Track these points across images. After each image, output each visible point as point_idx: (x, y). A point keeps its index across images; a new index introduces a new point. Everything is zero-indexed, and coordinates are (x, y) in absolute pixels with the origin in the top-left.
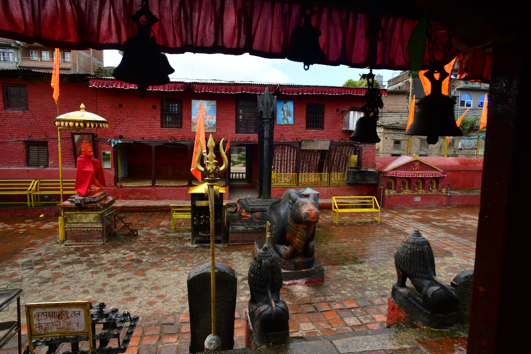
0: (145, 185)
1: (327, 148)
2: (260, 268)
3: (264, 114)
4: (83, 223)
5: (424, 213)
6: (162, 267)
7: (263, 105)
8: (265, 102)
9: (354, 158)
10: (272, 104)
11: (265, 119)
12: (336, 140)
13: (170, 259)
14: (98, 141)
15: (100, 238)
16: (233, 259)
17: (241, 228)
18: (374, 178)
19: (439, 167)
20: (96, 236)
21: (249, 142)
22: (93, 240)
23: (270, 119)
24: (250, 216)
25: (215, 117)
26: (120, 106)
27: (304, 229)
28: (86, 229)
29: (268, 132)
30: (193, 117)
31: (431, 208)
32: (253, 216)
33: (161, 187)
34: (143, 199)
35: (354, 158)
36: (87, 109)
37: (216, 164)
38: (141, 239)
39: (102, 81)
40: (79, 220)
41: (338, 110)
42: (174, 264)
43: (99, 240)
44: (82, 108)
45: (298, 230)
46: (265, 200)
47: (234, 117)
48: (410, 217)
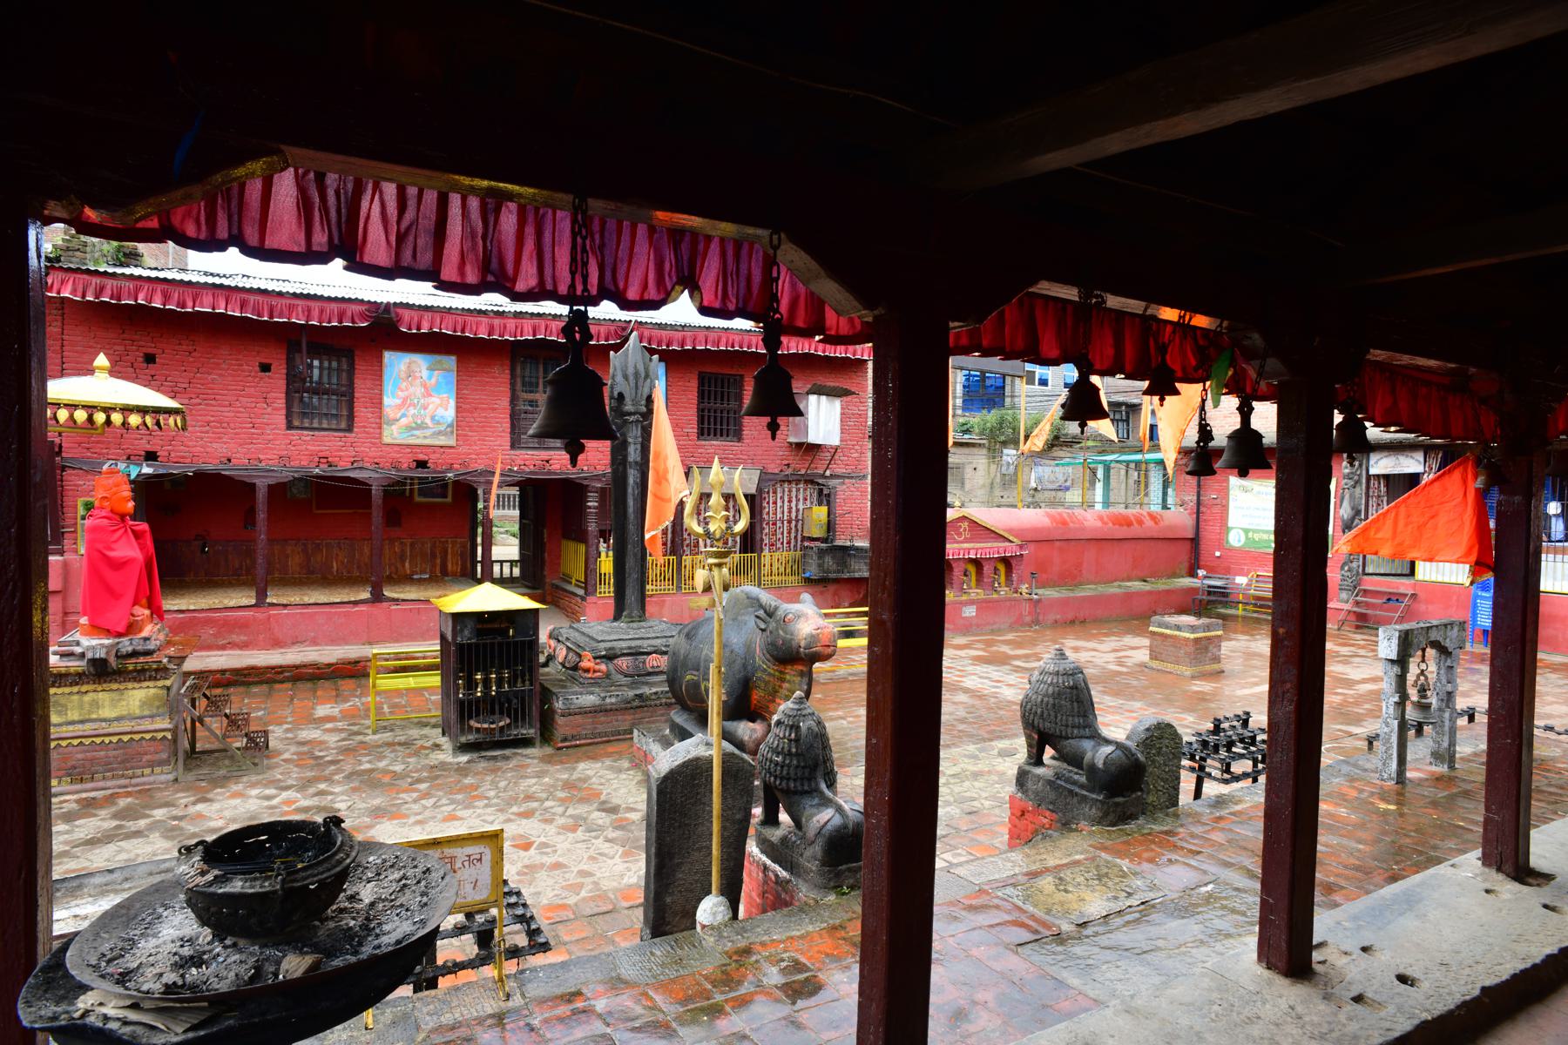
0: (232, 603)
2: (797, 740)
3: (628, 400)
4: (104, 720)
5: (989, 643)
6: (406, 816)
7: (626, 377)
8: (631, 371)
9: (821, 512)
10: (647, 376)
11: (630, 414)
12: (774, 468)
13: (415, 795)
14: (63, 468)
15: (161, 763)
16: (590, 778)
17: (589, 700)
19: (1010, 531)
20: (146, 758)
21: (549, 473)
22: (139, 772)
24: (603, 667)
25: (452, 403)
26: (150, 359)
27: (802, 674)
28: (115, 739)
30: (388, 401)
31: (999, 632)
32: (611, 666)
33: (285, 606)
34: (223, 648)
35: (821, 512)
36: (114, 372)
37: (727, 519)
38: (286, 756)
39: (96, 280)
40: (90, 712)
42: (435, 806)
43: (157, 770)
44: (102, 369)
45: (783, 680)
46: (635, 625)
47: (504, 403)
48: (962, 653)
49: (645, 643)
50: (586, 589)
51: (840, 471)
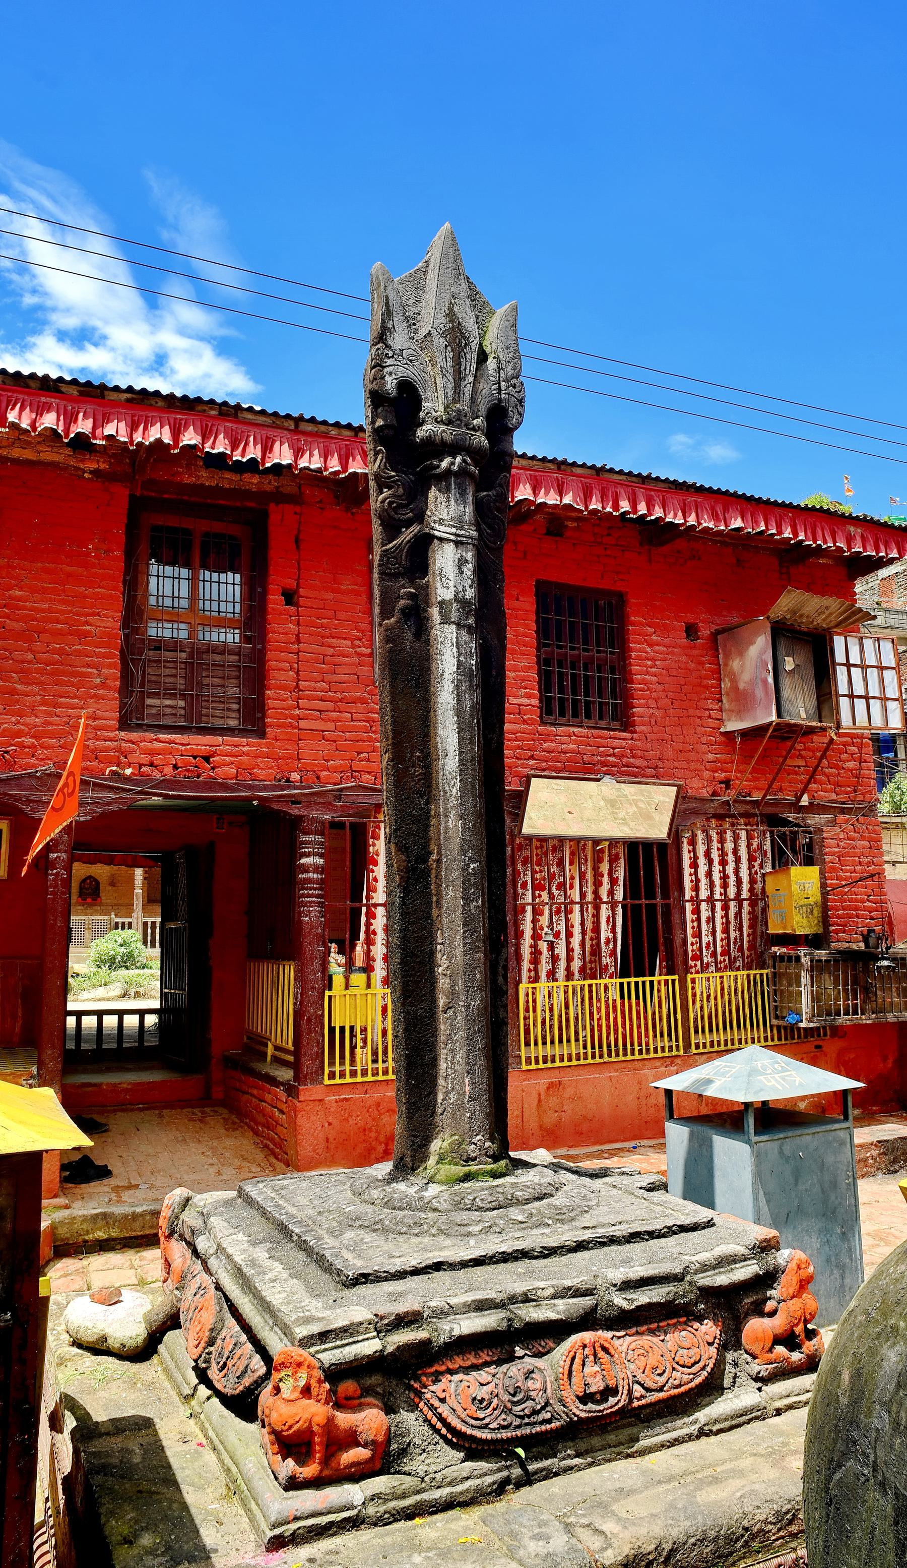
12: (700, 788)
21: (211, 785)
47: (109, 621)
50: (296, 1066)
51: (827, 796)
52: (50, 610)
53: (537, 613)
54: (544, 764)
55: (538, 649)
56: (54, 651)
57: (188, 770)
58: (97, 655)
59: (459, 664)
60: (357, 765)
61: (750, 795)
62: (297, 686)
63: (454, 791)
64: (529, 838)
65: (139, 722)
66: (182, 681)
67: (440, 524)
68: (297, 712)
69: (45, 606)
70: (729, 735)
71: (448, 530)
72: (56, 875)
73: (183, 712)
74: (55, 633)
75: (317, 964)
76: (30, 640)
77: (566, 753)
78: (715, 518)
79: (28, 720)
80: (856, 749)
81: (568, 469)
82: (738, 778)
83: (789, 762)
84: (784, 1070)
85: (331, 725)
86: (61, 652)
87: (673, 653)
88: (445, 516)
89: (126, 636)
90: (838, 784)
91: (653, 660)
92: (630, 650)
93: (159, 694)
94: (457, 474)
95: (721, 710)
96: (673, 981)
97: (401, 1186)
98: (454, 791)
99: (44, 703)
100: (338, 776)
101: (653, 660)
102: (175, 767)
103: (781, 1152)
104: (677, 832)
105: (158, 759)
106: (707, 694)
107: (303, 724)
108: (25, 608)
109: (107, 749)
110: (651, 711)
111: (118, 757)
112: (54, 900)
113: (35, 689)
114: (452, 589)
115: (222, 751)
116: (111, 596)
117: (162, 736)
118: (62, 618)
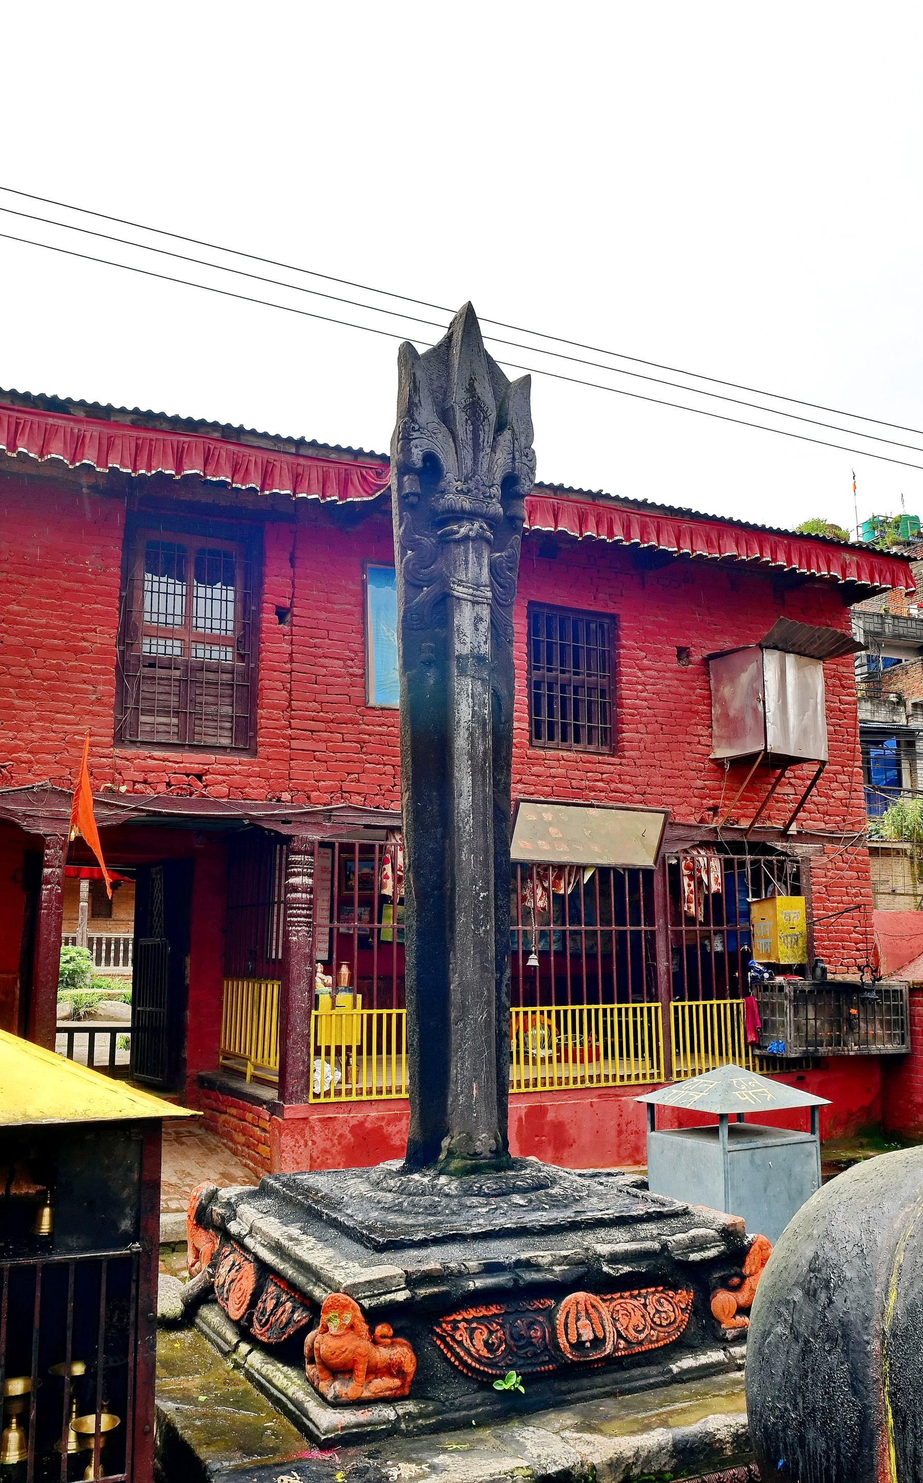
1: (646, 860)
11: (459, 516)
18: (888, 1025)
23: (492, 521)
29: (485, 612)
41: (682, 653)
47: (105, 637)
49: (542, 1253)
50: (282, 1086)
52: (46, 626)
53: (529, 634)
54: (532, 789)
55: (529, 672)
56: (51, 667)
57: (182, 789)
58: (92, 671)
59: (474, 713)
60: (347, 786)
61: (737, 823)
62: (290, 706)
63: (467, 827)
64: (516, 863)
65: (134, 739)
66: (174, 698)
67: (459, 585)
68: (289, 732)
69: (44, 621)
70: (719, 763)
71: (466, 590)
72: (51, 890)
73: (176, 730)
74: (54, 649)
75: (304, 984)
76: (26, 655)
77: (554, 777)
78: (709, 544)
79: (25, 735)
80: (846, 778)
81: (565, 496)
82: (726, 806)
83: (778, 789)
84: (757, 1087)
85: (322, 746)
86: (58, 667)
87: (664, 678)
88: (464, 578)
89: (123, 653)
90: (826, 813)
91: (644, 684)
92: (620, 673)
93: (153, 711)
94: (474, 540)
95: (711, 736)
96: (656, 1008)
97: (416, 1176)
98: (467, 827)
99: (41, 719)
100: (328, 796)
101: (644, 684)
102: (169, 785)
103: (752, 1162)
104: (664, 858)
105: (151, 777)
106: (697, 720)
107: (295, 744)
108: (23, 624)
109: (102, 766)
110: (640, 736)
111: (113, 774)
112: (48, 915)
113: (31, 703)
114: (469, 645)
115: (214, 769)
116: (107, 613)
117: (157, 754)
118: (59, 633)
